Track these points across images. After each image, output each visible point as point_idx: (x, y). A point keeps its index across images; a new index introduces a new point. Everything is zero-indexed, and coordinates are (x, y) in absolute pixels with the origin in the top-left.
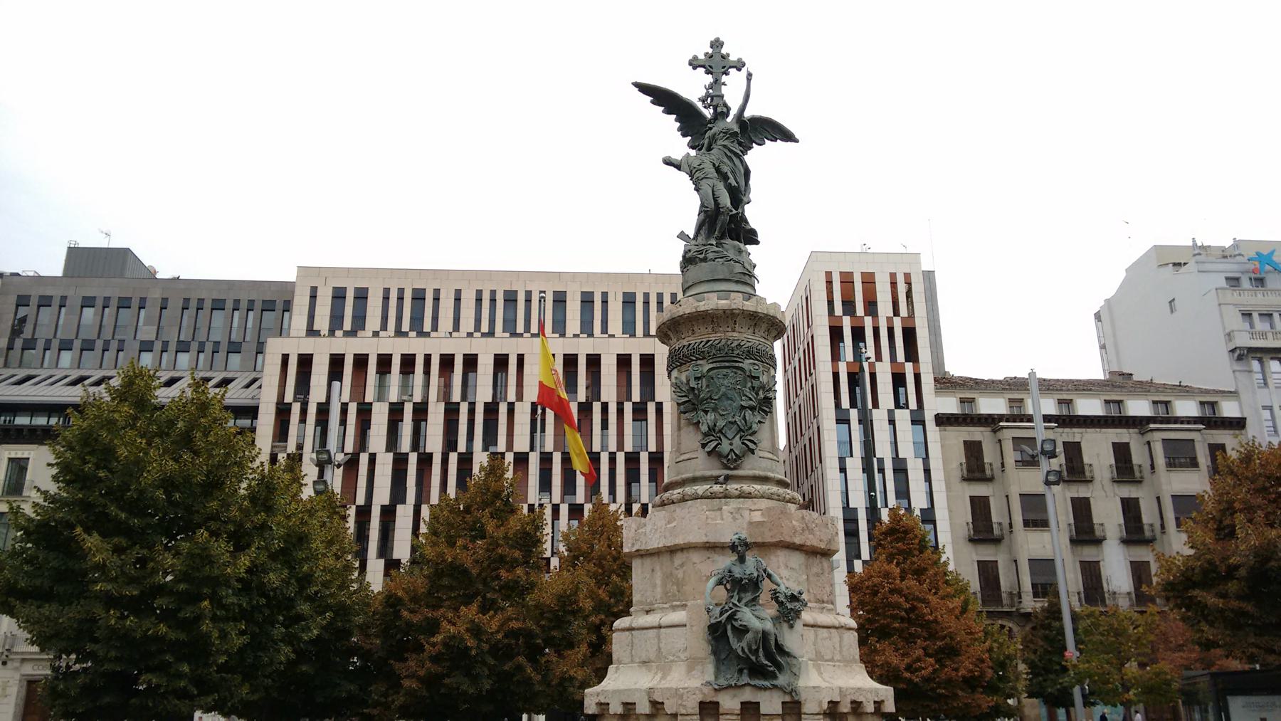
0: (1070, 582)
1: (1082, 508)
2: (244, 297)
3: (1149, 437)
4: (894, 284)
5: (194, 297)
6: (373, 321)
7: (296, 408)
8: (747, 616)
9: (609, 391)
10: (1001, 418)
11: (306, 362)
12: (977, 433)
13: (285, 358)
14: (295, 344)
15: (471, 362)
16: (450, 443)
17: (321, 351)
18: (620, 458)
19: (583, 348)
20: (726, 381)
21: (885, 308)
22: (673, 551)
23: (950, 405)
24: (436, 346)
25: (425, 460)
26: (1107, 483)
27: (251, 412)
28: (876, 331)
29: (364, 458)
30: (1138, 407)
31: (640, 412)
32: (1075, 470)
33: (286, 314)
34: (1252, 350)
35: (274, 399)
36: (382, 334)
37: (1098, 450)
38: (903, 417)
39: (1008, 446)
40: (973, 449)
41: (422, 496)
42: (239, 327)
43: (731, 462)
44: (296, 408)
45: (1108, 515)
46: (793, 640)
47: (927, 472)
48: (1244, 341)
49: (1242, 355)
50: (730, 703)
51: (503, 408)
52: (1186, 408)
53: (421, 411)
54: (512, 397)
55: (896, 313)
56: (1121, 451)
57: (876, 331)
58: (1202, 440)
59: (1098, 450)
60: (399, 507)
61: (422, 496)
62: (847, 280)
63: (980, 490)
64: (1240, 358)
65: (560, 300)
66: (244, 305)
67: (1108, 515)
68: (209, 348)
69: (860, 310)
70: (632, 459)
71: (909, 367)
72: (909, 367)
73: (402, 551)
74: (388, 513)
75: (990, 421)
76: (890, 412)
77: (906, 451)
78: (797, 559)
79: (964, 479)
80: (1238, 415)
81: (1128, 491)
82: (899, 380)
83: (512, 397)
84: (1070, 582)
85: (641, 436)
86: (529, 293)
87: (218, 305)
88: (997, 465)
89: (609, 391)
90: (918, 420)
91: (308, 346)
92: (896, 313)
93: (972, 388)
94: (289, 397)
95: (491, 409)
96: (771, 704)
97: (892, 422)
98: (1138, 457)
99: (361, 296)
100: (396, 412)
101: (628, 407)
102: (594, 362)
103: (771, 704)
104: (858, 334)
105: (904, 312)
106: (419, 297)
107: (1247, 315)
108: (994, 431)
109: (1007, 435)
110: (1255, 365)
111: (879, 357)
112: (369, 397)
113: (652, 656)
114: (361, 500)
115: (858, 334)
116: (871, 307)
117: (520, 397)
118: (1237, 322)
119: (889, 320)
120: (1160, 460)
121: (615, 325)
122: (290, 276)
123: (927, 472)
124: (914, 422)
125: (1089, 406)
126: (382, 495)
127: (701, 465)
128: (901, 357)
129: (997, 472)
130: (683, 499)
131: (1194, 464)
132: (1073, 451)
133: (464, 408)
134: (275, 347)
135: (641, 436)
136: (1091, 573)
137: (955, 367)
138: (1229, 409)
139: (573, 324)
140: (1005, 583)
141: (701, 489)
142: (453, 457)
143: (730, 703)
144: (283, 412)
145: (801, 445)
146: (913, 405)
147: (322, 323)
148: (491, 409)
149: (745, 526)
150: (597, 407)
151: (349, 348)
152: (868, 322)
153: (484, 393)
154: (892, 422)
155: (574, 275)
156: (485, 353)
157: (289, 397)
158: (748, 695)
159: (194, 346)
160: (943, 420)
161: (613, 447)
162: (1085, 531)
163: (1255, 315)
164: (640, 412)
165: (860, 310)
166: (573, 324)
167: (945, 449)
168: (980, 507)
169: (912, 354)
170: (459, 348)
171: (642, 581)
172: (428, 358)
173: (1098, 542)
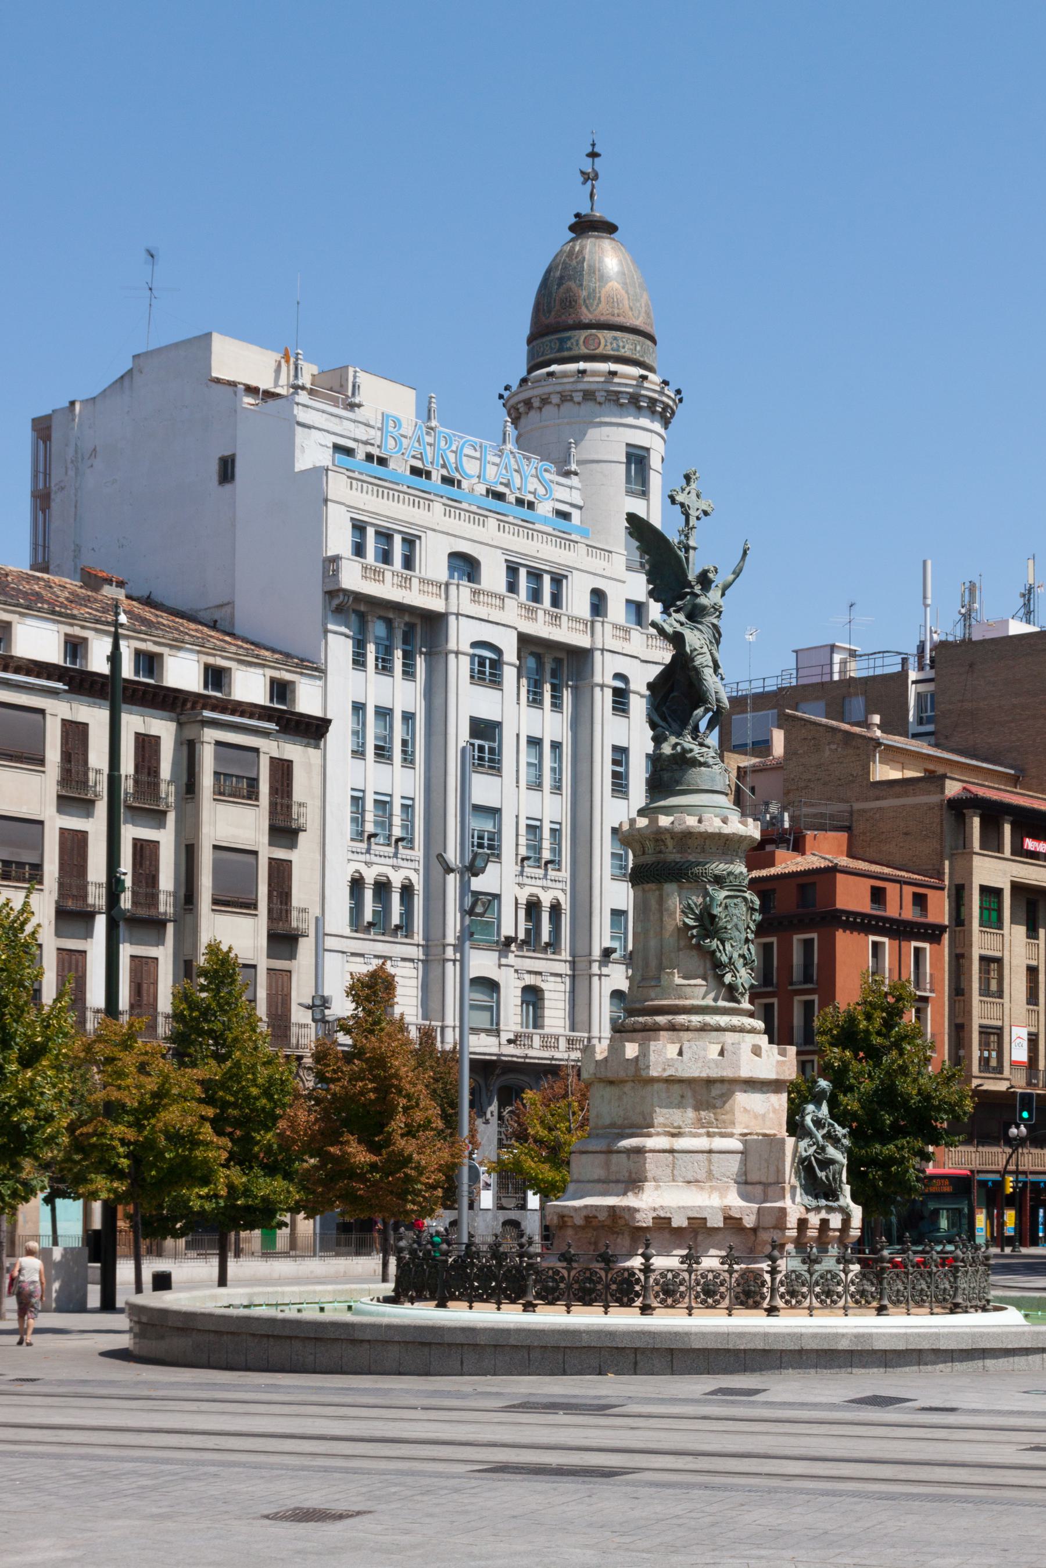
50: (814, 1220)
96: (836, 1221)
103: (836, 1221)
113: (702, 1175)
130: (704, 1028)
138: (307, 700)
141: (723, 1020)
143: (814, 1220)
149: (774, 1063)
158: (823, 1215)
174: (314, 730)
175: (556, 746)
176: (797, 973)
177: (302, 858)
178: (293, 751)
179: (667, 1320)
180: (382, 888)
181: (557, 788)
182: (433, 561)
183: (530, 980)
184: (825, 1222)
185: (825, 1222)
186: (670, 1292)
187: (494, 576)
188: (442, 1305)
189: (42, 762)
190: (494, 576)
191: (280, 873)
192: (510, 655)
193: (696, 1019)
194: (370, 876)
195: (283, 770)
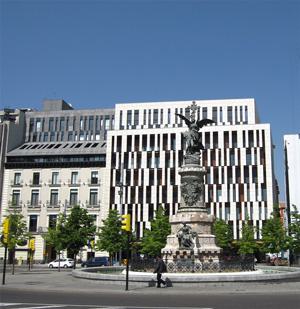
6: (141, 122)
7: (118, 154)
8: (185, 237)
9: (221, 144)
11: (120, 138)
14: (116, 133)
15: (173, 136)
17: (124, 134)
18: (226, 168)
24: (161, 131)
25: (160, 172)
27: (105, 155)
29: (140, 171)
41: (159, 183)
44: (118, 154)
50: (181, 252)
53: (157, 155)
70: (230, 169)
73: (154, 201)
74: (149, 189)
85: (232, 160)
89: (221, 144)
91: (120, 133)
96: (188, 252)
100: (149, 156)
101: (228, 150)
103: (188, 252)
112: (141, 149)
114: (140, 184)
121: (225, 119)
126: (146, 183)
133: (172, 152)
134: (110, 134)
135: (232, 160)
142: (169, 170)
143: (181, 252)
144: (114, 155)
147: (124, 123)
150: (217, 151)
151: (133, 133)
161: (223, 164)
164: (232, 152)
170: (169, 131)
184: (185, 253)
185: (185, 253)
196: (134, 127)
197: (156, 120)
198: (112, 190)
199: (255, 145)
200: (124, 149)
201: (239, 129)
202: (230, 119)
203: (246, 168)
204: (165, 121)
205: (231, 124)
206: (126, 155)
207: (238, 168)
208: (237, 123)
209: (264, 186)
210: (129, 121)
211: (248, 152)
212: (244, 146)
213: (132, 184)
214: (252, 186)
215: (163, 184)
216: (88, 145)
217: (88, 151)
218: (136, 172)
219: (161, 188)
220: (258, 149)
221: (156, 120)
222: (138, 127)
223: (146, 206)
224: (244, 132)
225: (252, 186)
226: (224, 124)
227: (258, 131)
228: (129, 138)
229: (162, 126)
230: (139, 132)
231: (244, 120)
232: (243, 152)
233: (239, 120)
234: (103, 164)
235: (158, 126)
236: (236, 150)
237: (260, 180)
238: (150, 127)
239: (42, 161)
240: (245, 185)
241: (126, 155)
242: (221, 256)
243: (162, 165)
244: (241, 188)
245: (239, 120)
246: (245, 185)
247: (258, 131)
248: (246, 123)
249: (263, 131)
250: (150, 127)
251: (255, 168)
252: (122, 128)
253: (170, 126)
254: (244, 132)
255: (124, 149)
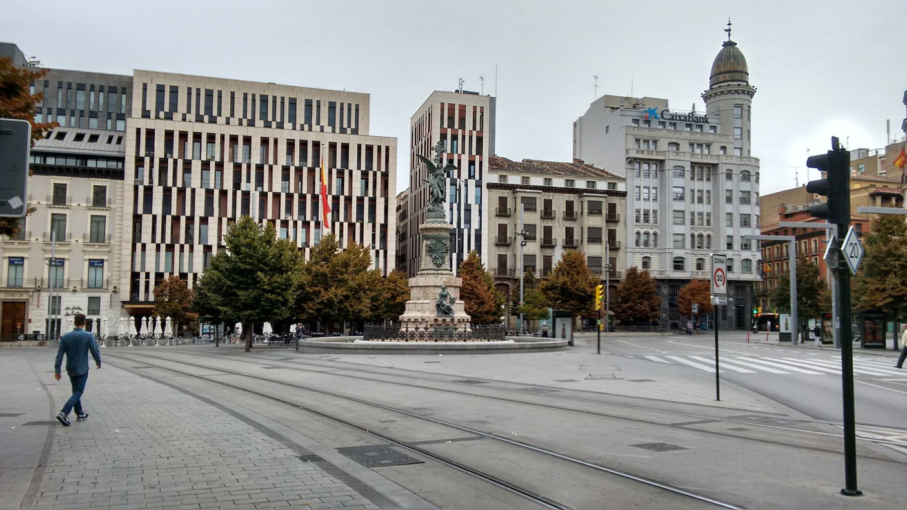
0: (539, 264)
1: (548, 231)
2: (97, 83)
3: (583, 199)
4: (475, 113)
5: (66, 80)
6: (182, 107)
8: (445, 303)
10: (518, 186)
11: (150, 133)
12: (505, 193)
13: (138, 131)
16: (237, 186)
17: (160, 127)
19: (310, 137)
20: (439, 246)
21: (469, 125)
22: (425, 286)
23: (494, 178)
26: (561, 220)
27: (122, 159)
28: (464, 137)
30: (580, 184)
31: (340, 174)
32: (548, 213)
33: (124, 96)
34: (635, 159)
35: (134, 154)
36: (188, 116)
37: (559, 203)
38: (472, 183)
39: (519, 200)
40: (503, 201)
41: (223, 212)
42: (95, 102)
43: (439, 266)
45: (559, 235)
46: (453, 307)
47: (480, 211)
48: (633, 154)
49: (631, 161)
50: (440, 319)
51: (266, 168)
52: (602, 185)
54: (271, 162)
55: (474, 128)
56: (570, 205)
57: (464, 137)
58: (605, 202)
59: (559, 203)
60: (210, 218)
61: (223, 212)
62: (452, 108)
63: (504, 221)
64: (630, 162)
65: (293, 103)
66: (97, 88)
67: (559, 235)
68: (77, 113)
69: (456, 126)
71: (477, 158)
72: (477, 158)
75: (512, 188)
76: (466, 181)
77: (472, 200)
78: (453, 289)
79: (497, 216)
80: (624, 190)
81: (569, 224)
82: (472, 163)
83: (271, 162)
84: (539, 264)
86: (275, 98)
87: (81, 87)
88: (513, 209)
90: (479, 185)
92: (474, 128)
93: (505, 170)
94: (142, 153)
95: (260, 168)
96: (448, 319)
97: (466, 185)
98: (576, 208)
99: (174, 91)
102: (316, 145)
103: (448, 319)
104: (454, 137)
105: (478, 129)
106: (209, 94)
107: (638, 140)
108: (514, 193)
109: (519, 195)
110: (637, 166)
111: (463, 152)
114: (188, 213)
115: (454, 137)
116: (462, 125)
117: (276, 162)
118: (632, 144)
119: (471, 132)
120: (586, 211)
121: (324, 121)
122: (131, 74)
123: (480, 211)
124: (476, 186)
125: (558, 182)
126: (200, 212)
127: (431, 266)
128: (474, 153)
129: (513, 212)
131: (600, 213)
132: (548, 204)
136: (548, 260)
137: (500, 153)
138: (621, 187)
139: (300, 119)
140: (509, 265)
141: (432, 272)
143: (440, 319)
145: (418, 191)
146: (477, 178)
147: (151, 106)
148: (260, 168)
152: (460, 132)
153: (256, 159)
154: (466, 185)
155: (301, 89)
156: (257, 133)
157: (142, 153)
159: (68, 112)
160: (491, 186)
162: (547, 243)
163: (642, 141)
165: (456, 126)
166: (300, 119)
167: (490, 200)
168: (502, 229)
169: (480, 152)
171: (414, 293)
172: (223, 137)
173: (553, 247)
174: (623, 194)
175: (708, 192)
176: (813, 250)
177: (619, 229)
178: (615, 200)
179: (411, 343)
180: (647, 234)
181: (709, 202)
182: (663, 145)
183: (699, 257)
186: (412, 336)
187: (685, 147)
188: (383, 340)
189: (535, 210)
190: (685, 147)
191: (612, 234)
192: (688, 167)
193: (426, 272)
194: (642, 231)
195: (612, 207)
196: (169, 117)
197: (209, 109)
198: (137, 219)
199: (375, 168)
200: (159, 151)
201: (353, 141)
202: (332, 122)
203: (360, 200)
204: (226, 112)
205: (334, 131)
206: (164, 162)
207: (348, 200)
208: (343, 131)
209: (384, 227)
210: (160, 105)
211: (365, 175)
212: (359, 168)
213: (174, 212)
214: (368, 227)
215: (230, 215)
216: (79, 137)
217: (84, 147)
218: (182, 192)
219: (225, 220)
220: (379, 175)
221: (209, 109)
222: (177, 116)
223: (199, 249)
224: (359, 147)
225: (368, 227)
226: (322, 127)
227: (379, 148)
228: (169, 134)
229: (221, 120)
230: (177, 126)
231: (353, 126)
232: (357, 174)
233: (345, 126)
234: (119, 175)
235: (213, 121)
236: (346, 173)
237: (380, 219)
238: (199, 119)
239: (102, 164)
240: (358, 225)
241: (164, 162)
242: (473, 323)
243: (228, 185)
244: (352, 226)
245: (345, 126)
246: (358, 225)
247: (379, 148)
248: (355, 132)
249: (387, 148)
250: (199, 119)
251: (373, 201)
252: (146, 115)
253: (234, 121)
254: (359, 147)
255: (159, 151)
